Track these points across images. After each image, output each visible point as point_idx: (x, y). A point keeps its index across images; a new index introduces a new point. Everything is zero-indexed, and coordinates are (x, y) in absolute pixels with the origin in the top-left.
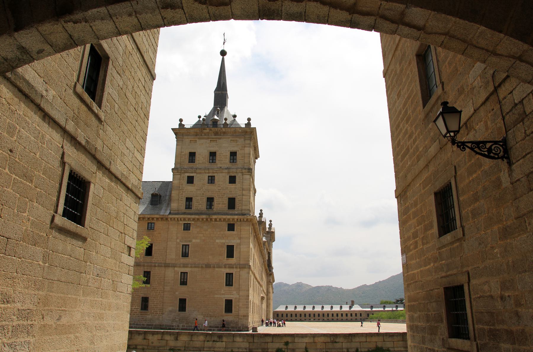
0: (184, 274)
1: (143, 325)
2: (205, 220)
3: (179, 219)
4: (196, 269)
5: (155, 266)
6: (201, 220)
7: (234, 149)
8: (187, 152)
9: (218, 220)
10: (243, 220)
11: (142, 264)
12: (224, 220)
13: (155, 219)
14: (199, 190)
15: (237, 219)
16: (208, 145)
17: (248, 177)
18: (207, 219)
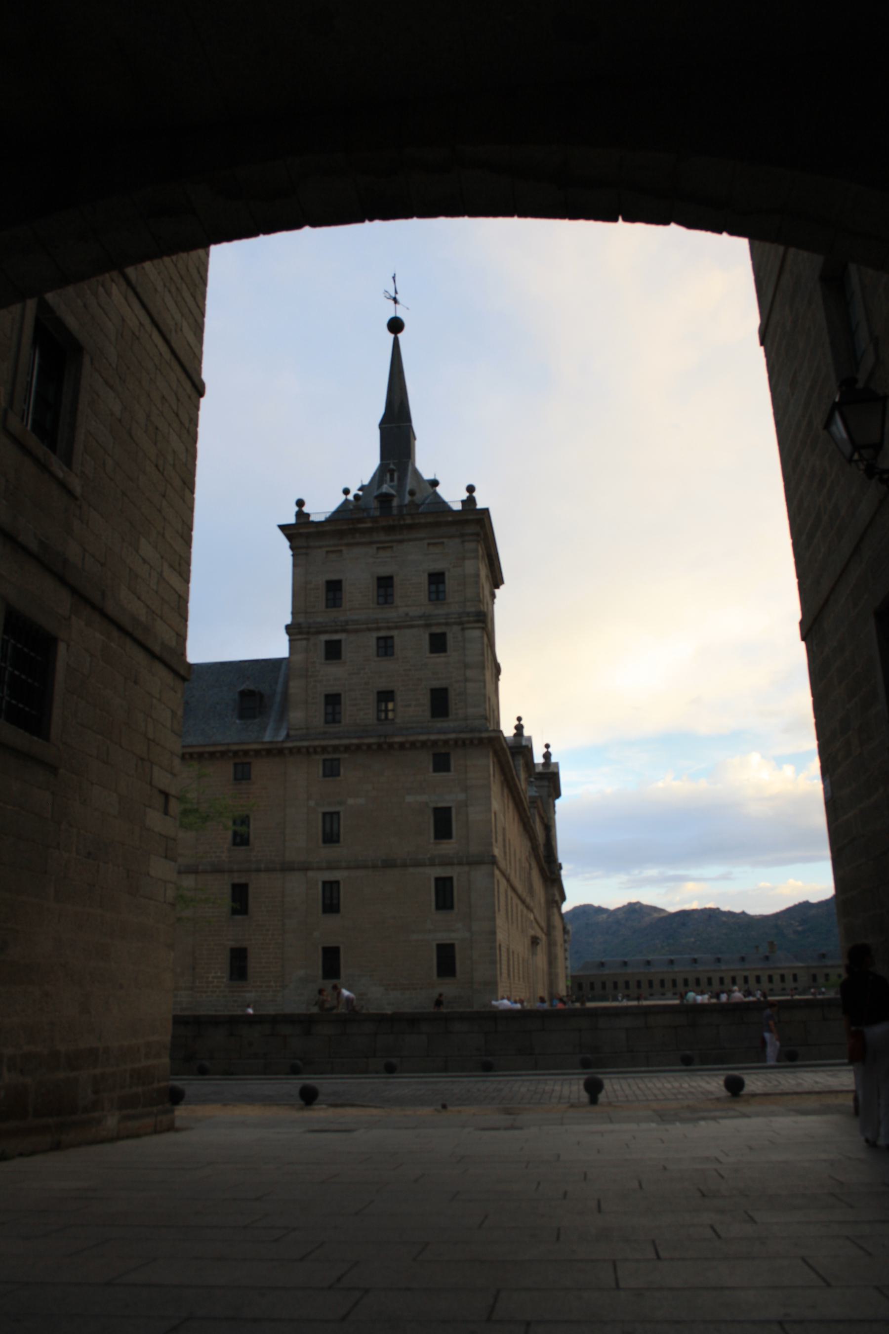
2: (374, 747)
3: (311, 750)
5: (258, 870)
7: (438, 566)
8: (320, 580)
9: (408, 745)
12: (424, 744)
14: (357, 672)
17: (477, 633)
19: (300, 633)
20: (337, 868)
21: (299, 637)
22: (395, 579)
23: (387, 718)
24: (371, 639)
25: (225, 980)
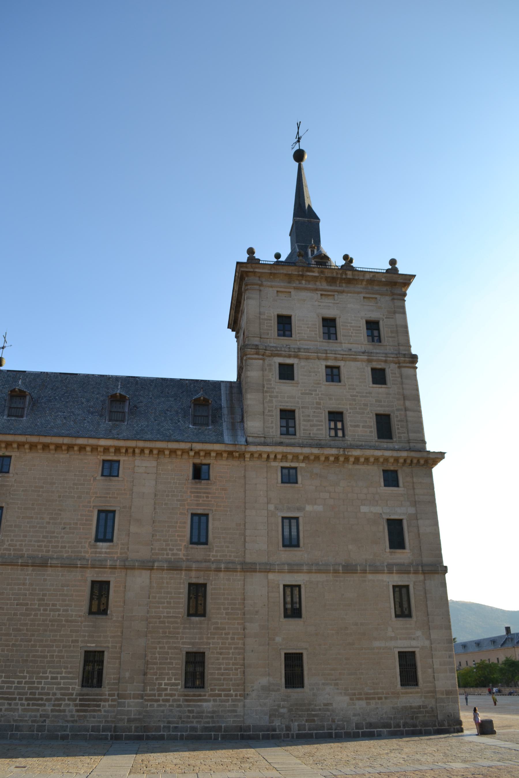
0: (292, 590)
1: (194, 729)
3: (272, 456)
4: (321, 578)
5: (218, 570)
6: (322, 458)
7: (374, 316)
9: (362, 460)
10: (418, 461)
11: (184, 565)
12: (377, 459)
13: (213, 454)
15: (405, 461)
16: (317, 303)
18: (337, 458)
19: (257, 354)
20: (299, 571)
21: (256, 356)
22: (338, 321)
23: (336, 435)
24: (321, 367)
25: (179, 687)
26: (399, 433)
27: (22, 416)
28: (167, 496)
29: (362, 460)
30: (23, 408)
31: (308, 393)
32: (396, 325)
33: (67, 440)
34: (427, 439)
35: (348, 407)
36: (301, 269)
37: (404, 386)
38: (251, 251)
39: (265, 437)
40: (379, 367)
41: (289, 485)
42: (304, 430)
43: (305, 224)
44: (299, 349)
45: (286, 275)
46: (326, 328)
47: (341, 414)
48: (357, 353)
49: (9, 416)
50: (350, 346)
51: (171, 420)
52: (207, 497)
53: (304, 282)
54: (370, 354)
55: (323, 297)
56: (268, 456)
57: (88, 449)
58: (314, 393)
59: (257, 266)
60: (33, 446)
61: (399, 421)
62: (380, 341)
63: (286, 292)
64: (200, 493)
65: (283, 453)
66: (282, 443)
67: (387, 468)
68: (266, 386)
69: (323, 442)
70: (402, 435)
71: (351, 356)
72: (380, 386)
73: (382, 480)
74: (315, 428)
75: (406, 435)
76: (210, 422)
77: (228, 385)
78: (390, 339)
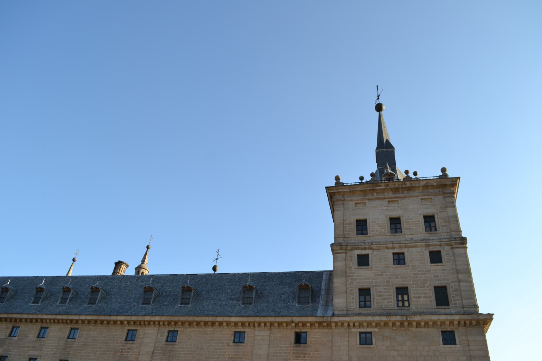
3: (351, 324)
6: (390, 324)
9: (423, 324)
10: (471, 323)
12: (435, 323)
13: (308, 325)
14: (381, 275)
15: (459, 323)
16: (385, 208)
18: (402, 324)
19: (341, 249)
23: (403, 305)
24: (389, 254)
26: (454, 300)
27: (189, 304)
28: (276, 356)
29: (423, 324)
30: (190, 298)
31: (381, 275)
32: (448, 217)
33: (210, 319)
34: (479, 304)
35: (411, 283)
36: (371, 185)
37: (457, 263)
38: (337, 178)
39: (347, 310)
40: (436, 250)
41: (366, 346)
42: (377, 303)
43: (385, 152)
44: (372, 242)
45: (361, 191)
46: (394, 225)
47: (406, 289)
48: (417, 241)
49: (181, 304)
50: (411, 236)
51: (284, 301)
52: (304, 357)
53: (375, 194)
54: (427, 240)
55: (390, 203)
56: (349, 325)
57: (225, 324)
58: (384, 274)
59: (343, 187)
60: (190, 324)
61: (454, 291)
62: (436, 230)
63: (362, 203)
64: (299, 354)
65: (359, 321)
66: (360, 313)
67: (445, 330)
68: (348, 272)
69: (392, 312)
70: (457, 302)
71: (413, 244)
72: (437, 264)
73: (441, 339)
74: (386, 301)
75: (460, 302)
76: (310, 301)
77: (329, 273)
78: (444, 228)
